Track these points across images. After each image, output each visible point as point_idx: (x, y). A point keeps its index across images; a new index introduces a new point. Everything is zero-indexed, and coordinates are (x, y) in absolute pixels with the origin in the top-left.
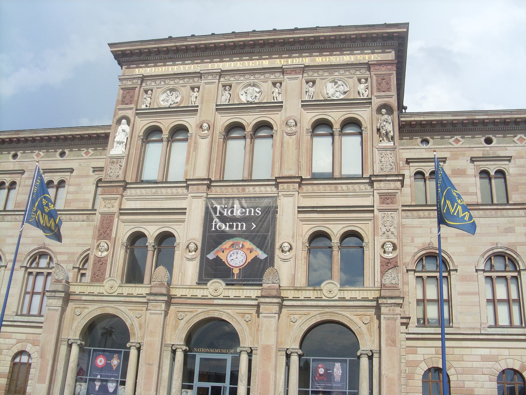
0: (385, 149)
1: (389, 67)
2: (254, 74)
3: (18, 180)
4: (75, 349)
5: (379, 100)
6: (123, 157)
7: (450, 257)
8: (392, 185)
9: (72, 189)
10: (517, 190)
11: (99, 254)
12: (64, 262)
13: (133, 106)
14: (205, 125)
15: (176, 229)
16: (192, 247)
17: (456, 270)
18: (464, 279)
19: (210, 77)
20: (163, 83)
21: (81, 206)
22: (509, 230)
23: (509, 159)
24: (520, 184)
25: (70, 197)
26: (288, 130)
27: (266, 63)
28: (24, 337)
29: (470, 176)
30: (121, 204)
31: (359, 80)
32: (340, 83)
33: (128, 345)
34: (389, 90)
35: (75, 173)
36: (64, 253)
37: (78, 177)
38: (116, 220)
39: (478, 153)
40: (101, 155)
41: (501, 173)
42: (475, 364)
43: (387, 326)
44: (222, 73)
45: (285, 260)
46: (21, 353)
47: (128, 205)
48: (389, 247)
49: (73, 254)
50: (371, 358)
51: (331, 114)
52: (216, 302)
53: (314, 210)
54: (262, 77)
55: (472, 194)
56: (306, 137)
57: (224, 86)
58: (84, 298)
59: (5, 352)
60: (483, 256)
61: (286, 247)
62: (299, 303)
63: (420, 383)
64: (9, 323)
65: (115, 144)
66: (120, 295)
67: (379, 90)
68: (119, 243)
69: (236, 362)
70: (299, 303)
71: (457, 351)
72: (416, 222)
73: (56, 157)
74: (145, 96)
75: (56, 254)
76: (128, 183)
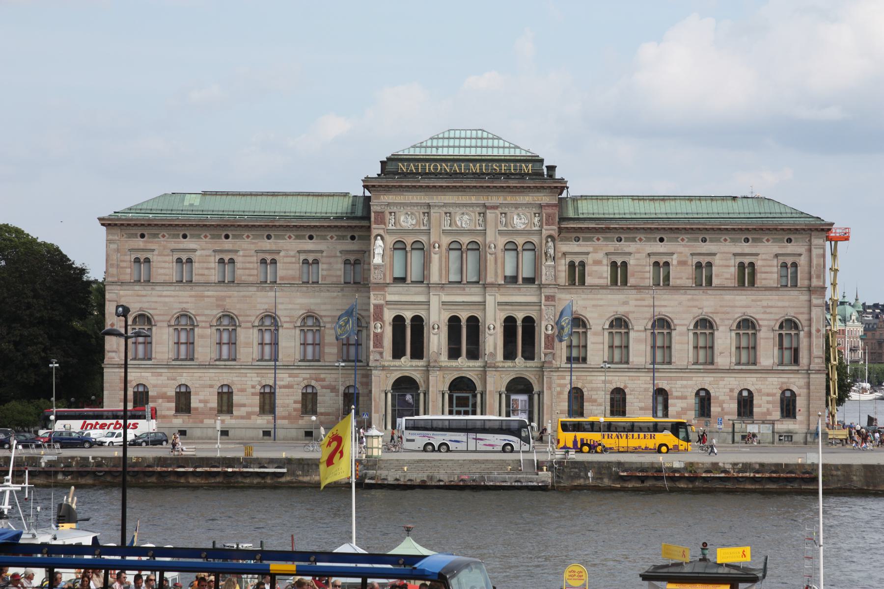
0: (549, 266)
1: (554, 208)
2: (466, 206)
3: (276, 257)
4: (389, 395)
5: (547, 232)
6: (383, 265)
7: (588, 320)
8: (552, 290)
9: (325, 266)
10: (634, 276)
11: (376, 331)
12: (329, 322)
13: (383, 226)
14: (437, 245)
15: (422, 314)
16: (436, 326)
17: (591, 329)
18: (595, 334)
19: (437, 208)
20: (402, 208)
21: (334, 280)
22: (626, 303)
23: (630, 254)
24: (637, 272)
25: (325, 273)
27: (473, 200)
28: (308, 376)
29: (604, 265)
30: (385, 297)
31: (535, 214)
32: (523, 216)
33: (419, 392)
34: (553, 224)
35: (324, 254)
36: (328, 316)
37: (327, 257)
38: (385, 310)
39: (611, 249)
40: (343, 240)
41: (625, 264)
42: (599, 385)
43: (547, 381)
44: (445, 205)
45: (491, 335)
46: (306, 386)
47: (389, 298)
48: (550, 328)
49: (335, 316)
50: (539, 395)
51: (517, 239)
52: (463, 369)
53: (507, 304)
54: (471, 209)
55: (604, 278)
56: (500, 255)
57: (446, 213)
58: (391, 368)
59: (295, 386)
60: (608, 319)
61: (492, 326)
62: (505, 369)
63: (567, 397)
64: (296, 367)
65: (376, 256)
66: (412, 366)
67: (546, 224)
69: (475, 396)
70: (505, 369)
71: (589, 378)
73: (305, 239)
75: (321, 316)
76: (388, 284)
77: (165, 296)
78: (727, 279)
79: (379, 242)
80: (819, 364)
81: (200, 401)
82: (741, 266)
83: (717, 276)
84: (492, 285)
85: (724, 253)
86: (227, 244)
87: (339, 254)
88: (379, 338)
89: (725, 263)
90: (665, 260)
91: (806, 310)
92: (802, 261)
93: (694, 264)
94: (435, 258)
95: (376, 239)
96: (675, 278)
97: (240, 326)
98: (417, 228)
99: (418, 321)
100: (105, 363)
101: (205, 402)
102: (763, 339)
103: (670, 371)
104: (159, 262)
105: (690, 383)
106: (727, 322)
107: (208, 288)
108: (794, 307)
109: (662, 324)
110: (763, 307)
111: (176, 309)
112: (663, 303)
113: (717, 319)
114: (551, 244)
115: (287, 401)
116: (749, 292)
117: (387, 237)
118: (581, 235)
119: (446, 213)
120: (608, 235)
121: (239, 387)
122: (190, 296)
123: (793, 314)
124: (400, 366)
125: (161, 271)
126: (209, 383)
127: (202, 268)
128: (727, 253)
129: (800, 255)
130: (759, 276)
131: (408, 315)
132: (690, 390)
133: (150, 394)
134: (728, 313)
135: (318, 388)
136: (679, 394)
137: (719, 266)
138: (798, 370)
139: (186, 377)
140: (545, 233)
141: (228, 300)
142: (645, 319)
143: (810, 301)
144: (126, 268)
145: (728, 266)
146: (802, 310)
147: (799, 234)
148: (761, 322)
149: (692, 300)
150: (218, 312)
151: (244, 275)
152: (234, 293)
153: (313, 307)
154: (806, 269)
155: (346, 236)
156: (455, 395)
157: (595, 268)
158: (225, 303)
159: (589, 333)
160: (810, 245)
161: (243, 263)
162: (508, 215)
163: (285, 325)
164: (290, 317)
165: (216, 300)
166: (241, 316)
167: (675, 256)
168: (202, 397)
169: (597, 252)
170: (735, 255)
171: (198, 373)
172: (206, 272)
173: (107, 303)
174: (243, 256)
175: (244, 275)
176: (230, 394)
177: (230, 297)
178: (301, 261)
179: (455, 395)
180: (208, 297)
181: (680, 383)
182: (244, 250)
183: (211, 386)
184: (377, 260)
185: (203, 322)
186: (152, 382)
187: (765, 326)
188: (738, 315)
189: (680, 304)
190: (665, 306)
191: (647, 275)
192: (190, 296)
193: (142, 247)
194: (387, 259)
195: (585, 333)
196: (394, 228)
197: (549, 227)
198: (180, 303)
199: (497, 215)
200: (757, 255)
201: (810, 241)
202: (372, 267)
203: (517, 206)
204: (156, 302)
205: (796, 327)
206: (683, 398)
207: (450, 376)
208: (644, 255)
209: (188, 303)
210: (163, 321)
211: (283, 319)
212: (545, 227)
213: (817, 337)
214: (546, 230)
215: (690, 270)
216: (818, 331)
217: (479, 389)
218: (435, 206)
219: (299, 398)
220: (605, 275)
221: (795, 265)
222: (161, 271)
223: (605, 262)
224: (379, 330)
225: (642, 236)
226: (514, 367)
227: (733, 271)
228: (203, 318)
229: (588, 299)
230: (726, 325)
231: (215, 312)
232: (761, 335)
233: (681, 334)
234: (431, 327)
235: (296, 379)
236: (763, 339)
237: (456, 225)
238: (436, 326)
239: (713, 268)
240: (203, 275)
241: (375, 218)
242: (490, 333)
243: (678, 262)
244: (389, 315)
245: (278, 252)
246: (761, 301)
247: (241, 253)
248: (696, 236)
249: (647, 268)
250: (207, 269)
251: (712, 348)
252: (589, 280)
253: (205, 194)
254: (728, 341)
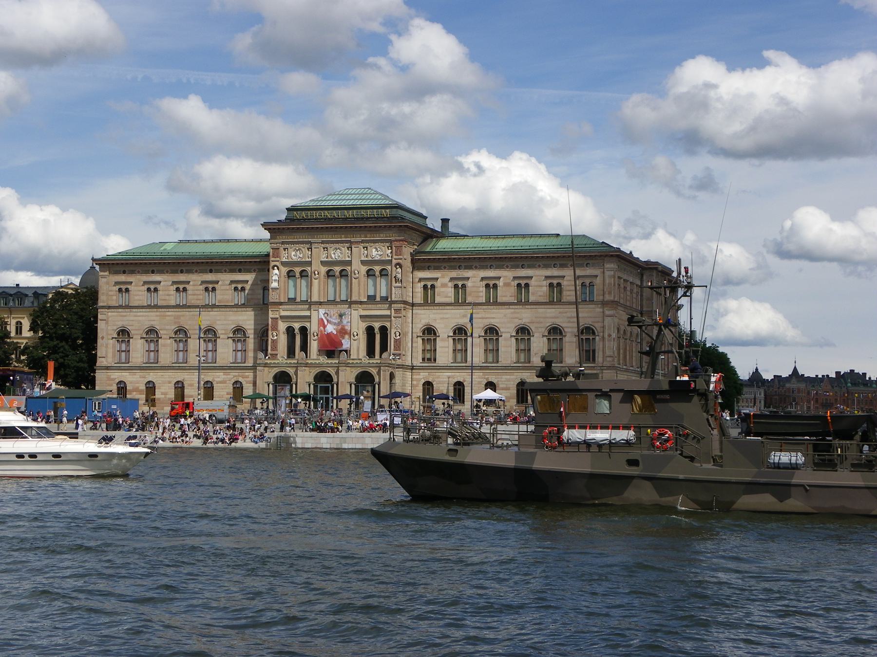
3: (216, 286)
13: (278, 259)
14: (316, 272)
15: (307, 325)
18: (443, 340)
19: (316, 245)
22: (465, 316)
23: (468, 278)
24: (475, 292)
26: (355, 276)
30: (279, 313)
31: (388, 247)
41: (464, 286)
42: (444, 379)
46: (236, 382)
47: (283, 313)
55: (449, 297)
67: (396, 255)
68: (281, 332)
72: (423, 312)
74: (284, 252)
77: (140, 316)
78: (540, 296)
79: (276, 271)
80: (610, 361)
81: (162, 394)
82: (551, 285)
83: (533, 294)
84: (356, 302)
85: (538, 276)
86: (182, 277)
87: (259, 283)
88: (274, 342)
89: (539, 283)
90: (494, 282)
91: (600, 319)
92: (598, 281)
93: (516, 285)
94: (315, 283)
95: (273, 269)
96: (502, 296)
97: (190, 338)
98: (304, 260)
99: (304, 330)
100: (97, 365)
101: (165, 394)
102: (568, 342)
103: (497, 368)
104: (135, 291)
105: (512, 377)
106: (540, 330)
107: (168, 310)
108: (591, 317)
109: (492, 332)
110: (568, 318)
111: (147, 325)
112: (493, 316)
113: (533, 327)
114: (399, 270)
115: (222, 393)
116: (556, 306)
117: (281, 267)
118: (432, 264)
119: (324, 248)
120: (452, 264)
121: (189, 382)
122: (157, 316)
123: (590, 323)
124: (278, 363)
125: (136, 298)
126: (168, 379)
127: (165, 295)
128: (542, 276)
129: (597, 276)
130: (564, 293)
131: (297, 326)
132: (512, 383)
133: (127, 388)
134: (541, 323)
135: (244, 383)
136: (504, 386)
137: (534, 286)
138: (594, 367)
139: (152, 376)
140: (394, 262)
141: (182, 318)
142: (479, 328)
143: (603, 312)
144: (113, 296)
145: (541, 286)
146: (597, 319)
147: (595, 259)
148: (566, 330)
149: (514, 313)
150: (174, 327)
151: (193, 299)
152: (186, 314)
153: (241, 324)
154: (601, 287)
155: (265, 269)
156: (319, 385)
157: (443, 290)
158: (180, 320)
159: (438, 339)
160: (604, 269)
161: (194, 290)
162: (369, 248)
163: (221, 336)
164: (225, 330)
165: (174, 318)
166: (190, 330)
167: (501, 279)
168: (163, 391)
169: (444, 278)
170: (547, 277)
171: (160, 373)
172: (167, 298)
173: (99, 321)
174: (193, 285)
175: (193, 299)
176: (183, 388)
177: (183, 316)
178: (233, 289)
179: (319, 385)
180: (169, 316)
181: (505, 377)
182: (195, 281)
183: (170, 382)
184: (274, 285)
185: (165, 334)
186: (129, 379)
187: (569, 332)
188: (548, 323)
189: (505, 316)
190: (494, 318)
191: (481, 294)
192: (157, 316)
193: (124, 280)
194: (282, 284)
195: (435, 340)
196: (287, 260)
197: (397, 257)
198: (151, 321)
199: (360, 249)
200: (564, 277)
201: (603, 265)
202: (270, 290)
203: (375, 242)
204: (133, 321)
205: (594, 333)
206: (507, 389)
207: (314, 371)
208: (479, 279)
209: (154, 321)
210: (137, 334)
211: (220, 332)
212: (394, 257)
213: (609, 341)
214: (395, 259)
215: (513, 290)
216: (610, 336)
217: (335, 380)
218: (315, 243)
219: (231, 390)
220: (450, 295)
221: (591, 285)
222: (136, 298)
223: (451, 284)
224: (276, 338)
225: (477, 264)
226: (361, 363)
227: (545, 289)
228: (165, 332)
229: (437, 313)
230: (539, 332)
231: (173, 327)
232: (566, 339)
233: (506, 339)
234: (312, 334)
235: (228, 376)
236: (568, 342)
237: (332, 258)
238: (315, 334)
239: (530, 288)
240: (164, 300)
241: (273, 254)
242: (354, 338)
243: (504, 283)
244: (282, 326)
245: (217, 282)
246: (566, 313)
247: (191, 283)
248: (518, 263)
249: (481, 289)
250: (169, 295)
251: (529, 350)
252: (438, 299)
253: (181, 242)
254: (542, 344)
